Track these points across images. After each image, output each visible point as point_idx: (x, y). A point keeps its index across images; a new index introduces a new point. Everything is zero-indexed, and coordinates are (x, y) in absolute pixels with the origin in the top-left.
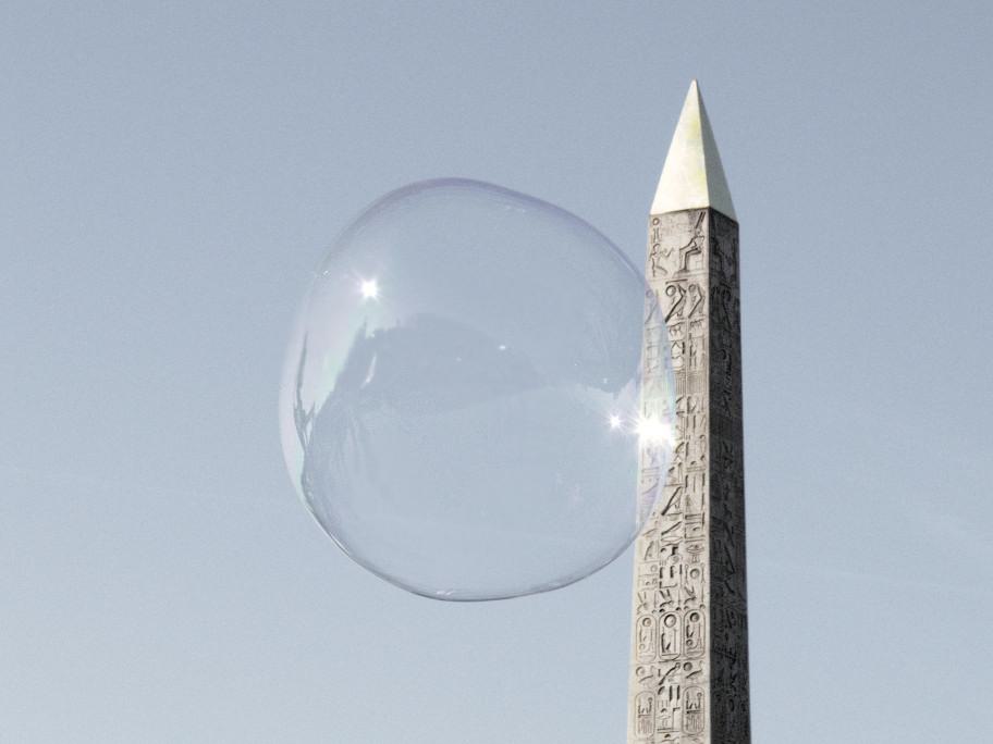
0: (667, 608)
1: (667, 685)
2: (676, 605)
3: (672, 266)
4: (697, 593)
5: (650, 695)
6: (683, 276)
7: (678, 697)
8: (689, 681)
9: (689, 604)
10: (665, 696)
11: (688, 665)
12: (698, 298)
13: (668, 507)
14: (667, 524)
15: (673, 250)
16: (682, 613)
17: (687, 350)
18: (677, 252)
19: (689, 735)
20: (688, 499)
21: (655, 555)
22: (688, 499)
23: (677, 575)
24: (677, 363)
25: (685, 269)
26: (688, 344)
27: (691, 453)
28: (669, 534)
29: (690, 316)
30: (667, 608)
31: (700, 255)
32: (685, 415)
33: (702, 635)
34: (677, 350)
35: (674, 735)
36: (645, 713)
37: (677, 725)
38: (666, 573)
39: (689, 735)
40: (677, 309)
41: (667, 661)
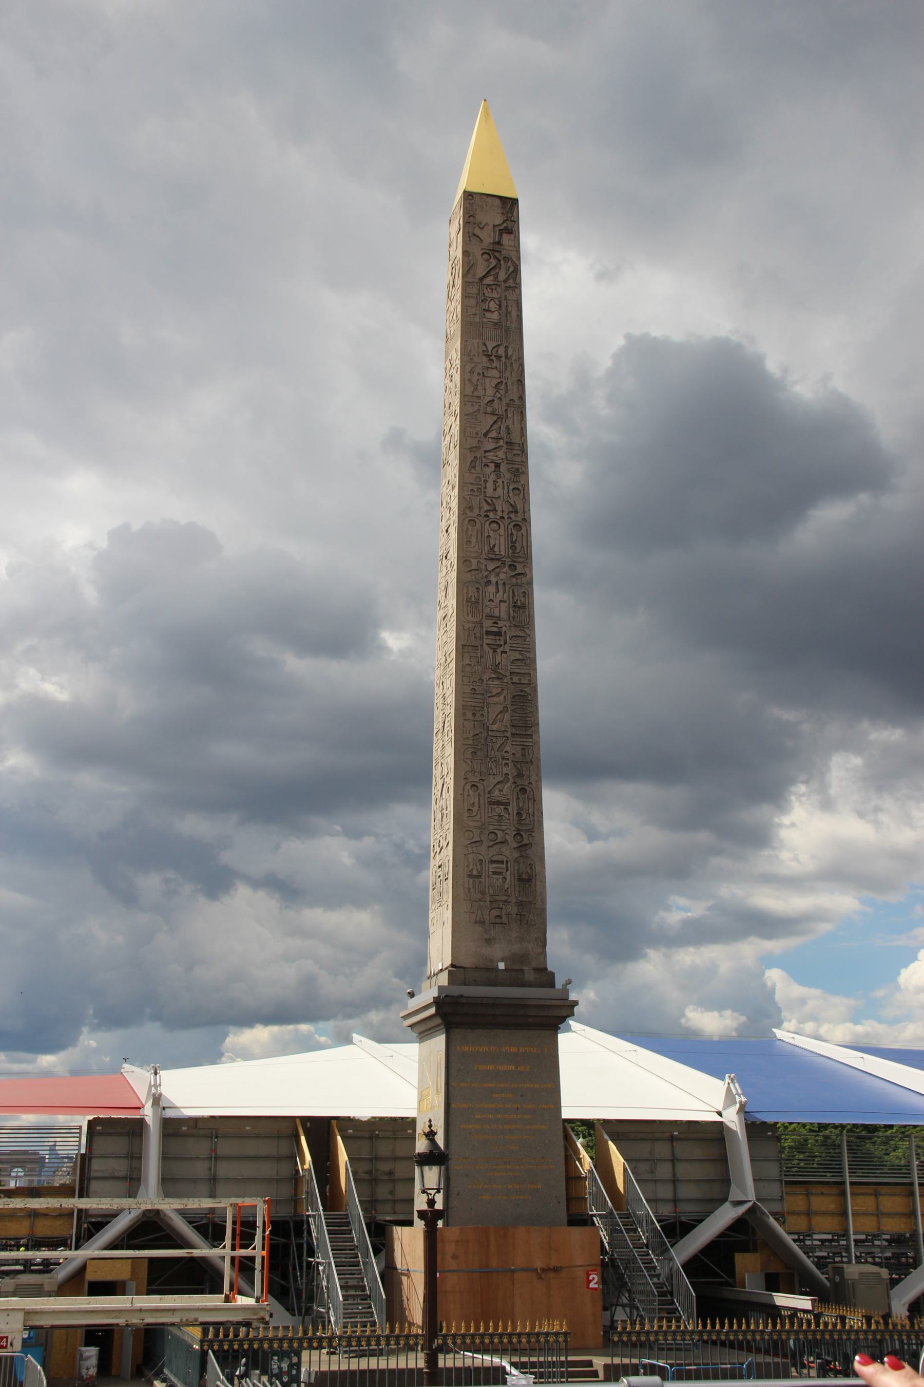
0: (491, 515)
1: (493, 579)
5: (477, 585)
6: (497, 247)
7: (505, 592)
8: (514, 580)
9: (512, 515)
10: (491, 589)
11: (513, 567)
12: (511, 269)
13: (488, 431)
15: (487, 224)
16: (507, 522)
17: (503, 308)
18: (491, 227)
19: (516, 626)
20: (508, 428)
21: (478, 469)
22: (508, 428)
23: (500, 490)
24: (495, 316)
25: (499, 243)
26: (504, 303)
27: (510, 392)
28: (491, 454)
29: (505, 281)
30: (491, 515)
31: (512, 236)
32: (503, 359)
33: (525, 544)
34: (493, 305)
35: (501, 624)
36: (473, 599)
37: (503, 615)
38: (490, 486)
39: (516, 626)
40: (493, 273)
41: (492, 559)
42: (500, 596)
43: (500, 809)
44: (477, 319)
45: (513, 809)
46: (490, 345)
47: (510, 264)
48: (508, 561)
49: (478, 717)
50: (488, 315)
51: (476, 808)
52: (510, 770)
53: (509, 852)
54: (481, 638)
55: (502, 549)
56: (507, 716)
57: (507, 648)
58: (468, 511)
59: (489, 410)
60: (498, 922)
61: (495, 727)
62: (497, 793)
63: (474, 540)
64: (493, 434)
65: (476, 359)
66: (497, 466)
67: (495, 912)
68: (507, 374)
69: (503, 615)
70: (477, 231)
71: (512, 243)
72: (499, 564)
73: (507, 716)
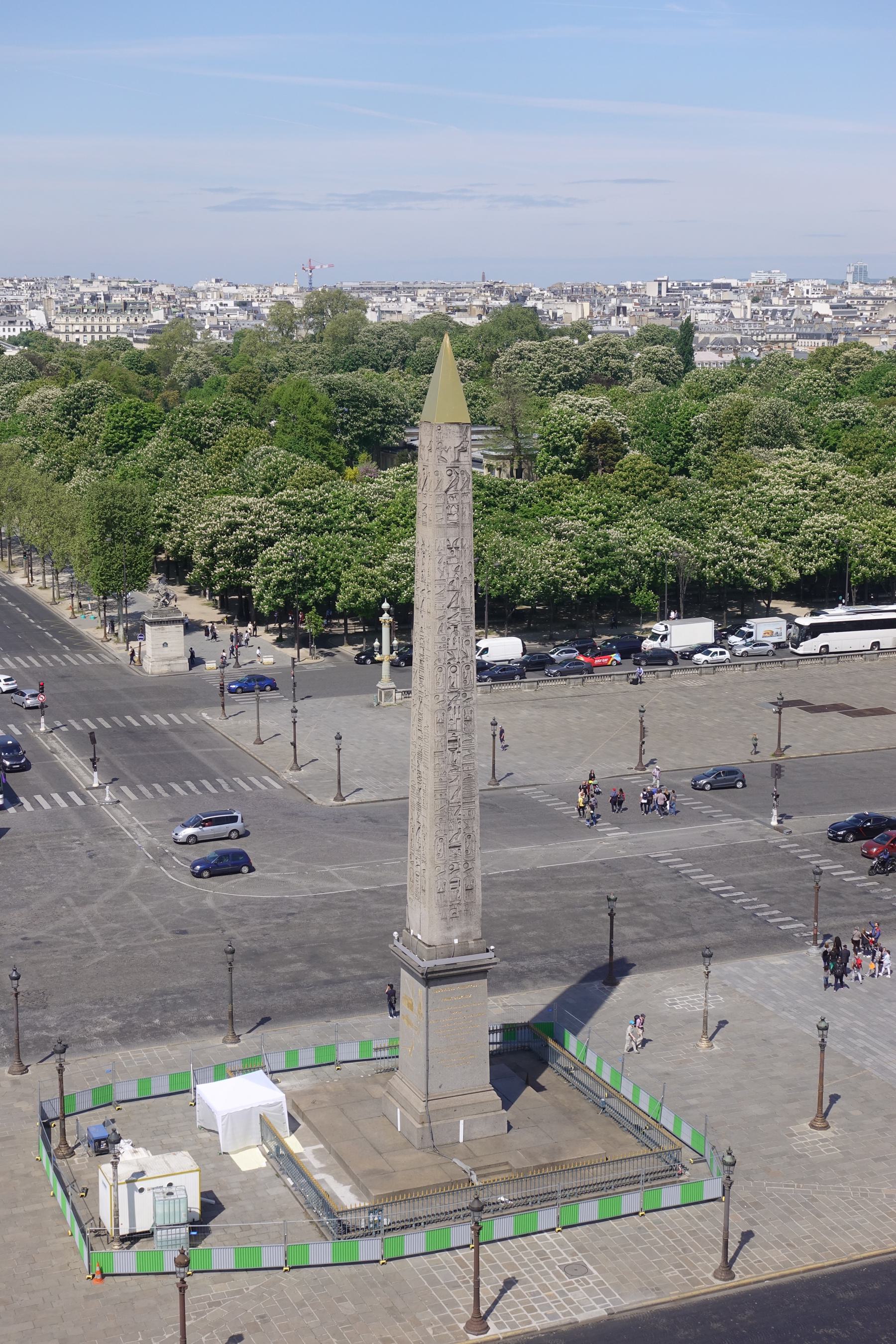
0: (452, 662)
1: (453, 705)
2: (457, 660)
3: (450, 457)
4: (469, 654)
6: (457, 464)
8: (465, 704)
9: (465, 660)
10: (451, 712)
11: (465, 695)
14: (451, 613)
16: (461, 664)
18: (452, 449)
20: (462, 599)
21: (444, 631)
22: (462, 599)
23: (457, 643)
24: (454, 518)
25: (458, 461)
26: (461, 506)
30: (452, 662)
34: (454, 510)
37: (459, 728)
38: (451, 642)
42: (456, 716)
43: (455, 850)
44: (443, 522)
45: (463, 849)
46: (451, 541)
47: (465, 476)
48: (462, 692)
49: (444, 796)
50: (450, 518)
51: (442, 853)
52: (462, 825)
53: (460, 875)
54: (445, 746)
55: (458, 684)
56: (460, 792)
57: (460, 749)
58: (437, 662)
59: (451, 588)
60: (454, 917)
61: (453, 801)
62: (454, 841)
63: (441, 681)
64: (453, 605)
65: (443, 553)
66: (456, 627)
67: (453, 911)
68: (462, 560)
69: (459, 728)
70: (444, 454)
71: (466, 459)
72: (456, 694)
73: (460, 792)
